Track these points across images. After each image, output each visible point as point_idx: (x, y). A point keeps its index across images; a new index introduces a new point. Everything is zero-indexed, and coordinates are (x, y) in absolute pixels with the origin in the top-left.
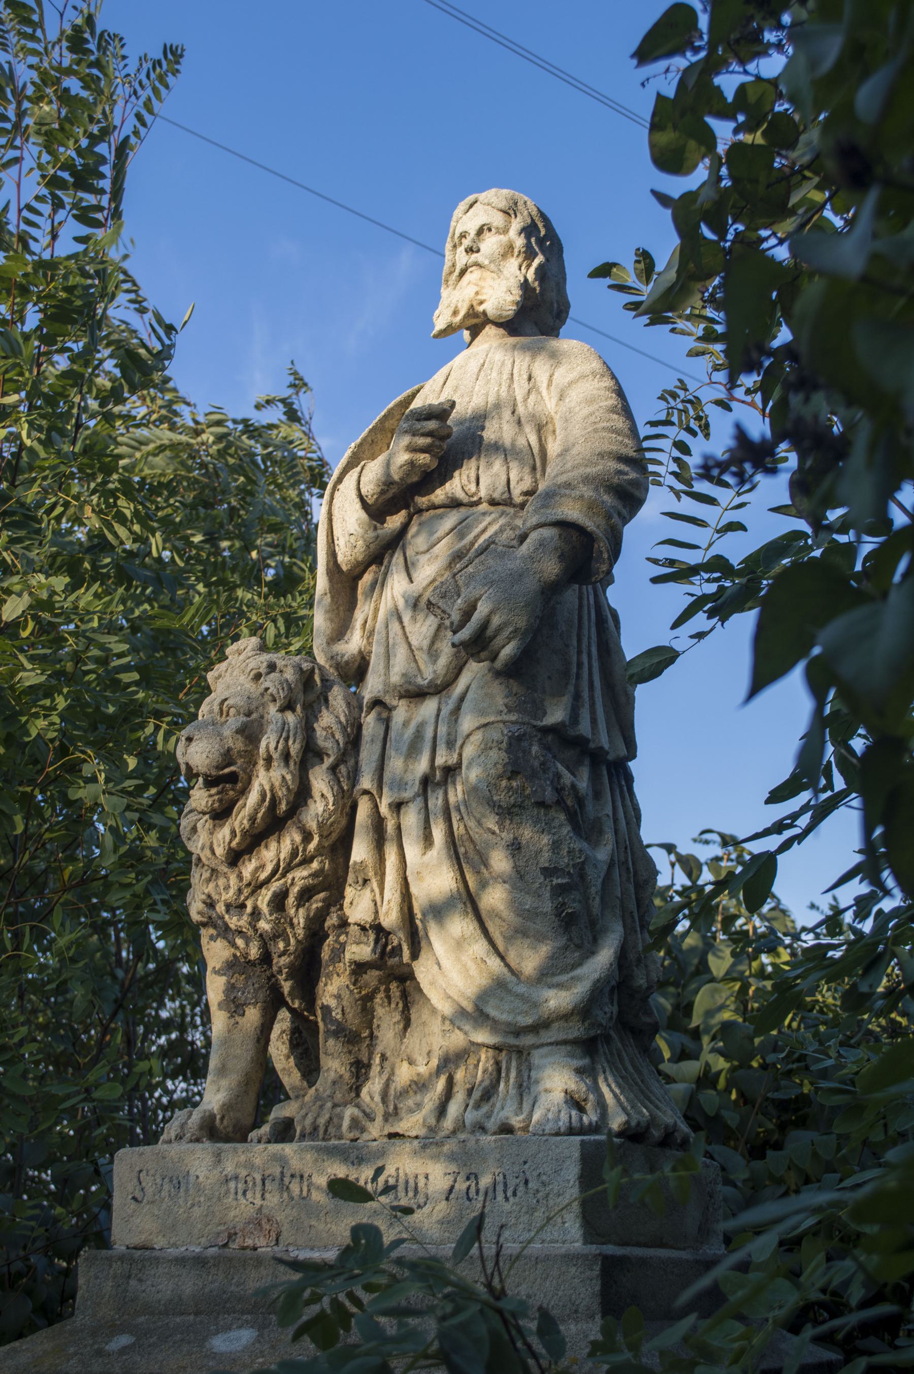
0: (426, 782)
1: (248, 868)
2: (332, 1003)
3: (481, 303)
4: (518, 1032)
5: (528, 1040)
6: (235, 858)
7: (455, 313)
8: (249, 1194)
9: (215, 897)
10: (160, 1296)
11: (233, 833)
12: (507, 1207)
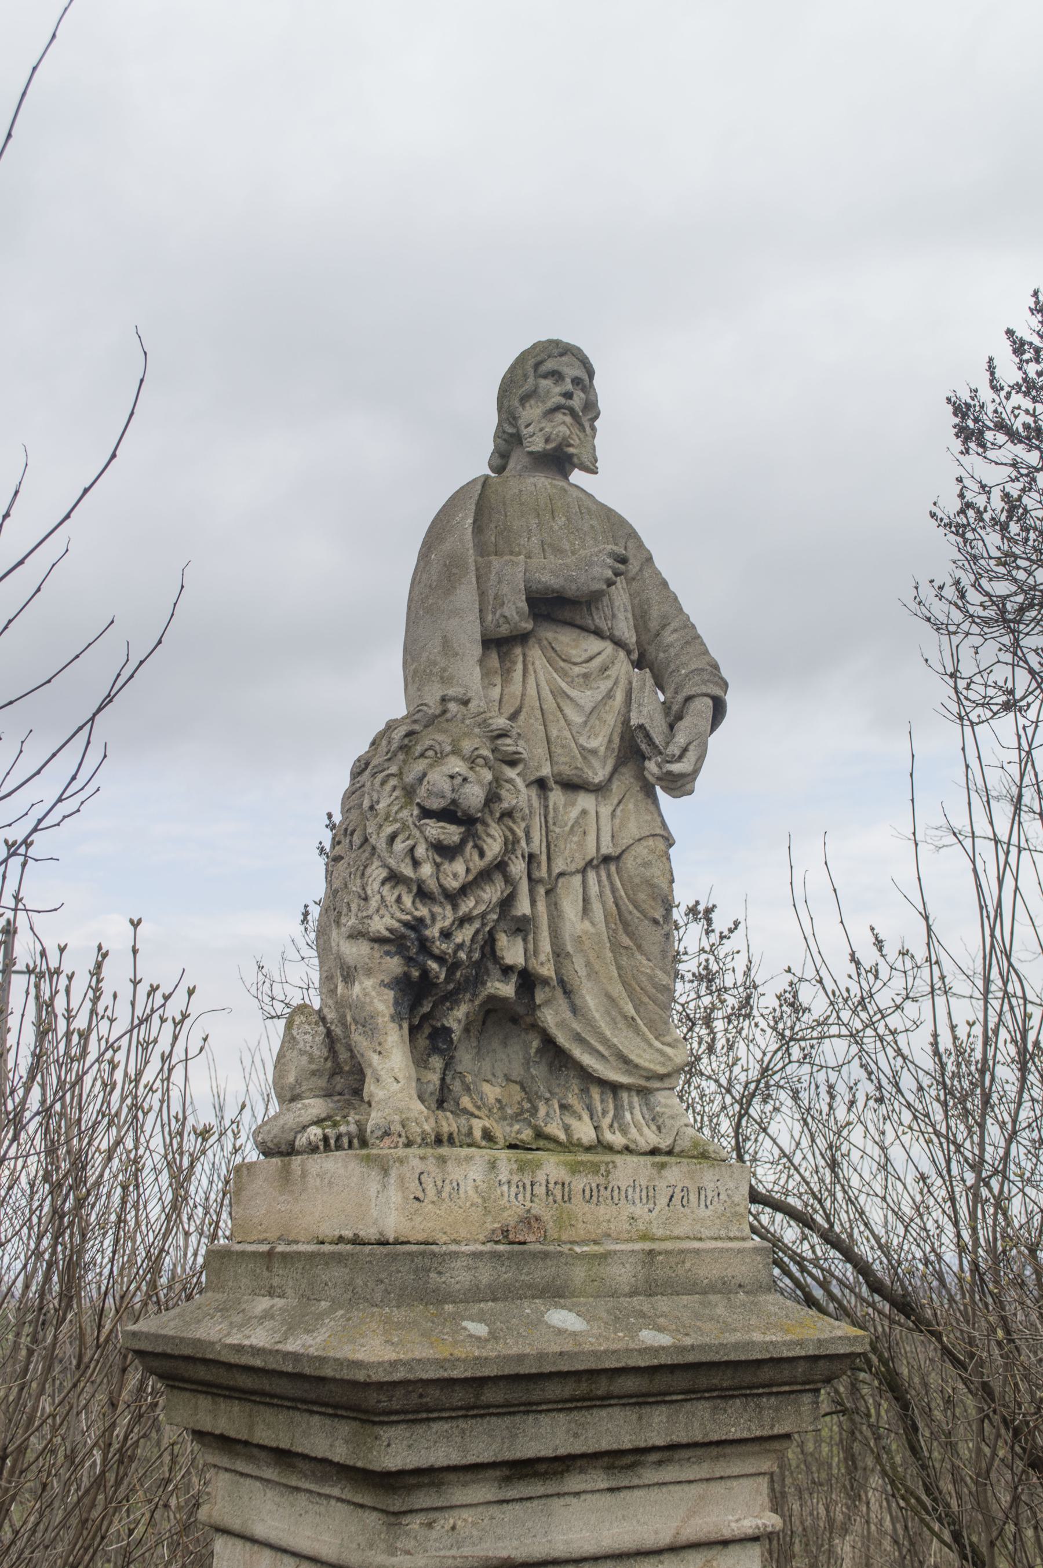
1: (468, 905)
2: (455, 1026)
3: (570, 445)
5: (657, 1084)
8: (521, 1197)
9: (428, 922)
10: (458, 1286)
11: (468, 870)
12: (708, 1213)
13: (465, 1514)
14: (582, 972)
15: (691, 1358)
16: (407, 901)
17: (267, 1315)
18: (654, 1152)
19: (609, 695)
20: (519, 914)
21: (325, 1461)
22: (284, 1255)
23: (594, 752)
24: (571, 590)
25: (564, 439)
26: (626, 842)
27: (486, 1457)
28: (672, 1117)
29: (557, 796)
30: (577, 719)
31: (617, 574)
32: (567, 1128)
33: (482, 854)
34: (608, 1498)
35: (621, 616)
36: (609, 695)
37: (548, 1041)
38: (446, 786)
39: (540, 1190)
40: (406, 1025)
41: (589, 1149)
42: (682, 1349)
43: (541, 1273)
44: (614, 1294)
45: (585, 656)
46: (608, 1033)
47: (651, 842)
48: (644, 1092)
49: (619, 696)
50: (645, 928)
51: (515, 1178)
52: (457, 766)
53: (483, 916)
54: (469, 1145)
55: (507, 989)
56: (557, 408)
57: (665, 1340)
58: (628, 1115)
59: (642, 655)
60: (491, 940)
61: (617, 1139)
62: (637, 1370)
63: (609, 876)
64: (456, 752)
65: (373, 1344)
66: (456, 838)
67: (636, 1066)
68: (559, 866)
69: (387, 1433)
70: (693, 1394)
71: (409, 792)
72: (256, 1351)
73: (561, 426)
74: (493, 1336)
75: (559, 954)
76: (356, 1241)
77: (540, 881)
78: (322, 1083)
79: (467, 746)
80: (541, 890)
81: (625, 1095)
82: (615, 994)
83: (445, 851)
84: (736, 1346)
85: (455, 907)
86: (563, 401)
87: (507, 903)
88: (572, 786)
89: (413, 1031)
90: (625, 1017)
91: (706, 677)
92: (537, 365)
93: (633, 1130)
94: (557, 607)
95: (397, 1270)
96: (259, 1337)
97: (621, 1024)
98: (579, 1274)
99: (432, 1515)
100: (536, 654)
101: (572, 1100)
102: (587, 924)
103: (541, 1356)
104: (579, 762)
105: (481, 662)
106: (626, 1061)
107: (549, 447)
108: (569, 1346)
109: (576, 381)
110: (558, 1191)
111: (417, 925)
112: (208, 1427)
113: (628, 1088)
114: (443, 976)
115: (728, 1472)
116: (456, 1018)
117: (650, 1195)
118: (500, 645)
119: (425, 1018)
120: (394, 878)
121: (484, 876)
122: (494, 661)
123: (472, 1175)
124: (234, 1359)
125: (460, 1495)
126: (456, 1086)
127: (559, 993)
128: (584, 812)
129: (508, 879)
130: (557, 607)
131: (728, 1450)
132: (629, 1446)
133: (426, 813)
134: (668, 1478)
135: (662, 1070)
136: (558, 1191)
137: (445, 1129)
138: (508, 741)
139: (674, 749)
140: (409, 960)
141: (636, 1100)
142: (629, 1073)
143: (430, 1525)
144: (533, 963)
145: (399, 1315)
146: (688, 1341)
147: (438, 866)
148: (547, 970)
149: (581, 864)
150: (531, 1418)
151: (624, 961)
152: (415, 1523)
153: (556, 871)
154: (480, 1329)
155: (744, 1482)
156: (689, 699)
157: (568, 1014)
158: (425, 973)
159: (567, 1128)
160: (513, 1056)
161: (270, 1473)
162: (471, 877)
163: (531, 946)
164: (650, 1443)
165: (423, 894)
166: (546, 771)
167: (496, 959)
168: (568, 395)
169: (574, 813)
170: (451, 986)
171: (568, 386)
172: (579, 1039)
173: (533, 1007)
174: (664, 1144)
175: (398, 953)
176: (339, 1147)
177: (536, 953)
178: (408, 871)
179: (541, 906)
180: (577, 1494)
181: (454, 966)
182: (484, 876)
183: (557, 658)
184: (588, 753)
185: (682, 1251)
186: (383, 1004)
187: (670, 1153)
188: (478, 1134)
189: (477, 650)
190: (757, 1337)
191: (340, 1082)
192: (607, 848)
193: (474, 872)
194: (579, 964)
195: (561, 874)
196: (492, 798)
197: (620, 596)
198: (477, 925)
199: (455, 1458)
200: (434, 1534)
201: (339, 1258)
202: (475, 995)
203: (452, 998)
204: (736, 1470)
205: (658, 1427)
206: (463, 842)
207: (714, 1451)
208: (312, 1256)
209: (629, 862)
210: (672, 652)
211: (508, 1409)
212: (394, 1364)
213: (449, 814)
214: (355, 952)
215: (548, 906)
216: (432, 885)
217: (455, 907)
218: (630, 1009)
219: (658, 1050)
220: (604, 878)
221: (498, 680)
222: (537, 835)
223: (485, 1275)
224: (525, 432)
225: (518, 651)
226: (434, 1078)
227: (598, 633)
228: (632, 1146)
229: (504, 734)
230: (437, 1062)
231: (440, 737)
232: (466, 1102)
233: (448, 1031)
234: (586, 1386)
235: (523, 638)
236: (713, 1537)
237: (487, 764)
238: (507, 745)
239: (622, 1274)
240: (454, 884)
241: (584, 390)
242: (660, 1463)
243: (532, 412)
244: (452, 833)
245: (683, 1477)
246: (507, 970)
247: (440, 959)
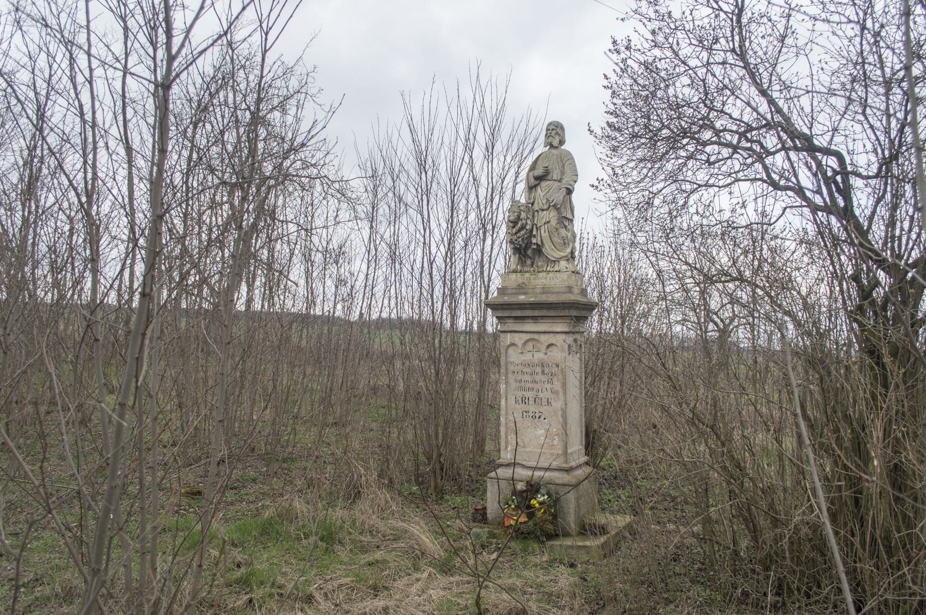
6: (516, 233)
43: (523, 291)
55: (535, 247)
70: (541, 308)
83: (513, 227)
88: (543, 210)
94: (540, 179)
116: (529, 252)
117: (546, 278)
148: (539, 243)
205: (536, 313)
223: (514, 291)
234: (521, 306)
239: (538, 291)
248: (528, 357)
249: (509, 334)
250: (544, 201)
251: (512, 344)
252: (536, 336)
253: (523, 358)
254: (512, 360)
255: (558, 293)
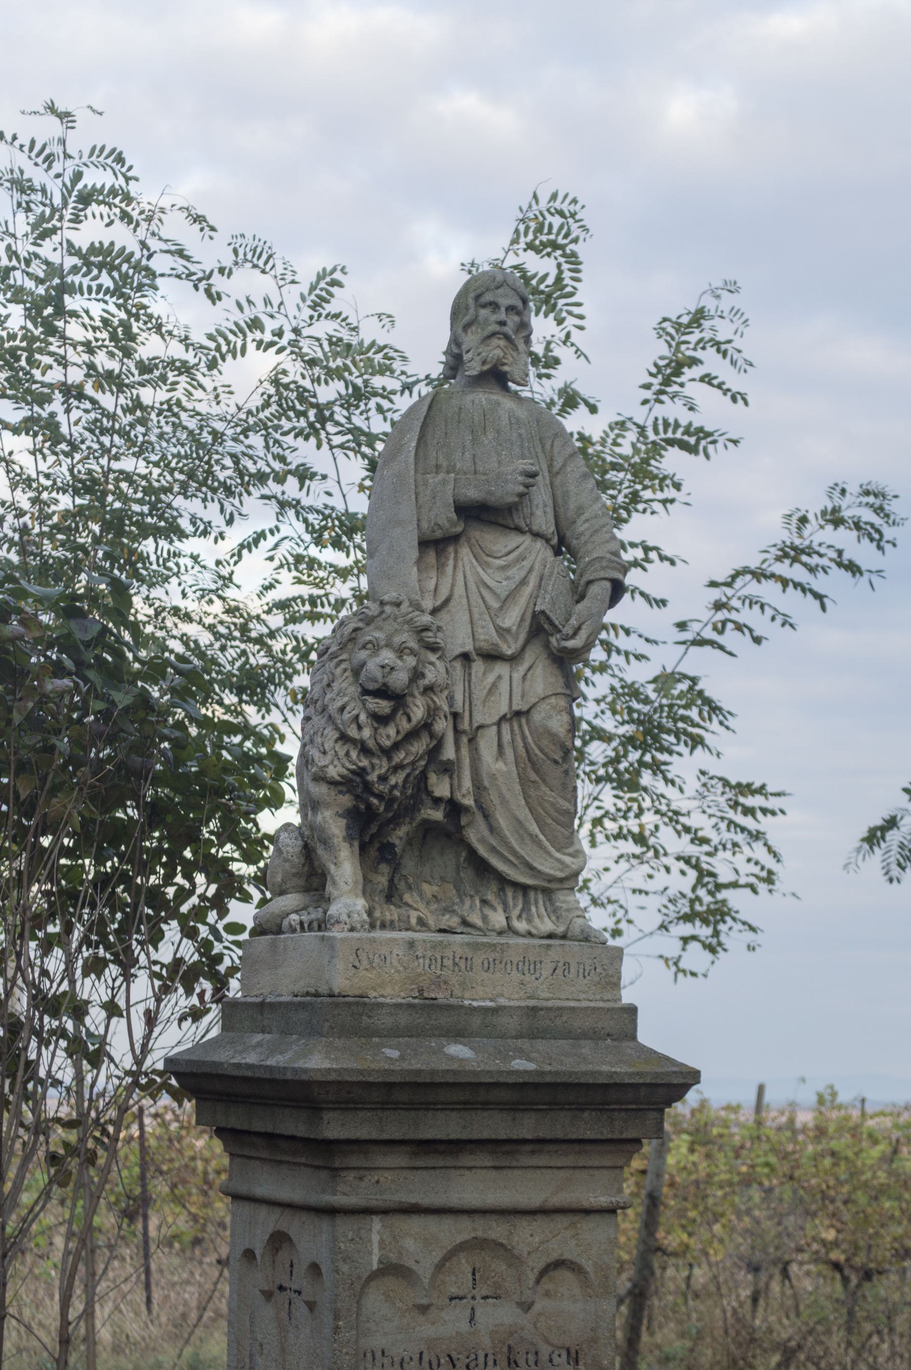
0: (503, 718)
1: (399, 757)
2: (397, 842)
4: (551, 879)
7: (484, 363)
11: (398, 732)
13: (388, 1174)
14: (496, 801)
15: (548, 1079)
16: (354, 754)
17: (259, 1044)
18: (551, 936)
19: (523, 582)
20: (445, 758)
21: (293, 1138)
22: (271, 1005)
23: (508, 630)
24: (492, 500)
25: (499, 360)
26: (533, 700)
27: (397, 1136)
28: (568, 910)
29: (478, 666)
30: (495, 604)
31: (527, 486)
32: (485, 918)
33: (409, 720)
34: (493, 1174)
35: (539, 513)
36: (523, 582)
37: (472, 853)
38: (378, 674)
39: (448, 963)
40: (356, 844)
41: (500, 933)
42: (542, 1073)
44: (503, 1036)
45: (505, 551)
46: (517, 848)
47: (553, 700)
48: (547, 892)
49: (533, 581)
50: (548, 767)
51: (429, 954)
52: (387, 656)
53: (413, 763)
54: (407, 930)
55: (437, 815)
56: (493, 334)
57: (531, 1066)
58: (533, 909)
59: (562, 541)
60: (424, 777)
61: (521, 926)
62: (506, 1085)
63: (520, 726)
64: (388, 645)
65: (317, 1060)
66: (388, 710)
67: (539, 872)
68: (479, 719)
69: (327, 1116)
71: (356, 672)
72: (250, 1066)
73: (495, 350)
74: (402, 1058)
75: (478, 786)
76: (317, 995)
77: (464, 732)
78: (301, 882)
79: (397, 640)
80: (465, 739)
81: (532, 895)
82: (522, 818)
84: (585, 1073)
85: (390, 759)
86: (497, 328)
87: (434, 752)
88: (492, 656)
89: (363, 848)
90: (531, 835)
91: (604, 564)
92: (478, 297)
93: (537, 920)
94: (481, 514)
95: (341, 1014)
96: (251, 1058)
97: (527, 841)
98: (476, 1021)
99: (362, 1172)
100: (465, 552)
101: (490, 897)
102: (500, 765)
103: (433, 1072)
104: (496, 638)
105: (419, 561)
106: (531, 868)
107: (486, 368)
108: (455, 1066)
109: (511, 309)
110: (462, 964)
111: (361, 772)
112: (223, 1125)
113: (535, 888)
114: (382, 808)
115: (590, 1163)
116: (399, 836)
118: (436, 545)
119: (373, 837)
120: (344, 738)
121: (412, 735)
122: (431, 557)
123: (395, 951)
124: (236, 1073)
125: (381, 1161)
126: (402, 886)
127: (479, 817)
128: (499, 677)
129: (432, 736)
130: (481, 514)
131: (589, 1147)
132: (504, 1137)
133: (366, 692)
134: (540, 1164)
135: (560, 874)
136: (462, 964)
137: (388, 917)
138: (430, 634)
139: (568, 630)
140: (357, 797)
141: (540, 897)
142: (534, 877)
143: (361, 1179)
144: (458, 796)
145: (339, 1042)
146: (548, 1068)
147: (376, 729)
148: (469, 801)
149: (496, 719)
150: (430, 1113)
151: (532, 792)
152: (351, 1176)
153: (475, 725)
154: (394, 1054)
155: (605, 1172)
156: (589, 583)
157: (486, 833)
158: (369, 806)
159: (485, 918)
160: (446, 862)
161: (264, 1154)
162: (400, 737)
163: (456, 782)
164: (521, 1137)
165: (365, 750)
166: (469, 647)
167: (429, 793)
168: (502, 323)
169: (491, 678)
170: (390, 815)
171: (502, 316)
172: (493, 850)
173: (460, 828)
174: (561, 929)
175: (349, 791)
176: (310, 929)
177: (460, 786)
178: (353, 732)
179: (465, 751)
180: (470, 1168)
181: (391, 801)
182: (412, 735)
183: (482, 556)
184: (502, 632)
185: (560, 1009)
186: (336, 828)
187: (564, 937)
188: (413, 921)
189: (414, 554)
190: (605, 1068)
191: (316, 881)
192: (519, 705)
193: (403, 733)
194: (493, 796)
195: (481, 727)
196: (417, 675)
197: (541, 495)
198: (407, 771)
199: (374, 1135)
200: (363, 1184)
201: (301, 1005)
202: (412, 819)
203: (395, 821)
204: (597, 1163)
205: (526, 1126)
206: (394, 711)
207: (577, 1147)
208: (290, 1003)
209: (537, 716)
210: (583, 539)
211: (411, 1107)
212: (329, 1070)
213: (383, 692)
214: (320, 790)
215: (470, 751)
216: (371, 744)
217: (390, 759)
218: (534, 829)
219: (557, 860)
220: (516, 728)
221: (433, 574)
222: (459, 697)
223: (404, 1019)
224: (466, 357)
225: (451, 549)
226: (382, 880)
227: (518, 530)
228: (534, 931)
229: (426, 629)
230: (384, 868)
231: (377, 634)
232: (407, 898)
233: (393, 846)
234: (472, 1093)
235: (455, 539)
236: (574, 1206)
237: (413, 653)
238: (429, 636)
240: (388, 743)
241: (519, 313)
242: (533, 1152)
243: (470, 339)
244: (383, 706)
245: (552, 1164)
246: (437, 801)
247: (380, 797)
248: (450, 1323)
249: (377, 1223)
250: (511, 619)
251: (394, 1269)
252: (496, 1230)
253: (426, 1330)
254: (377, 1342)
255: (595, 1036)
